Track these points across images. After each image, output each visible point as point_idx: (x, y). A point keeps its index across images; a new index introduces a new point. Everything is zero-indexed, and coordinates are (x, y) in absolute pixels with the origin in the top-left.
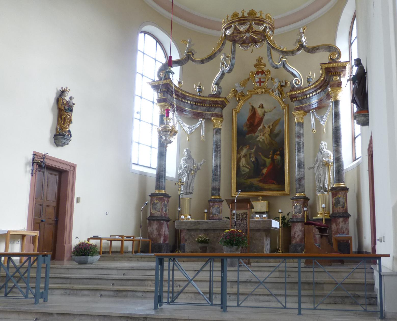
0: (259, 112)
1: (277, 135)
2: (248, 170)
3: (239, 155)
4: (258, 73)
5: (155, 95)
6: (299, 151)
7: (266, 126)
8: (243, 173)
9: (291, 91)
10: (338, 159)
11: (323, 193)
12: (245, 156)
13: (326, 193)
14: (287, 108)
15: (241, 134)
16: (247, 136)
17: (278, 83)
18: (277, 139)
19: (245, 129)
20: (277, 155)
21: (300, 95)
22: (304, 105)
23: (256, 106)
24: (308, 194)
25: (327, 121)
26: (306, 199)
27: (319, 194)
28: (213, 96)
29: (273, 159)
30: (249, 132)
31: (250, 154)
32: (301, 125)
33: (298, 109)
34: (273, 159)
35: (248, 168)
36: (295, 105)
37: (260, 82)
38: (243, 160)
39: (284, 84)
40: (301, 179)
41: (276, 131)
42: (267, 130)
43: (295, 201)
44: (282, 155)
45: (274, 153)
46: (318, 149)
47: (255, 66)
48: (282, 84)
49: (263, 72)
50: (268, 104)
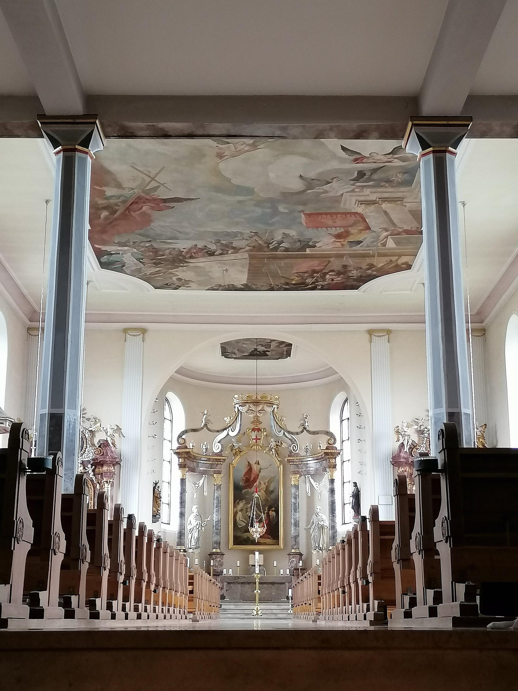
0: (255, 468)
1: (272, 492)
2: (245, 524)
3: (235, 509)
4: (254, 430)
5: (176, 460)
6: (295, 511)
7: (261, 483)
8: (240, 527)
9: (289, 456)
10: (333, 527)
11: (318, 552)
12: (241, 510)
13: (321, 551)
14: (282, 466)
15: (237, 489)
16: (243, 491)
17: (274, 443)
18: (273, 496)
19: (241, 484)
20: (273, 511)
21: (297, 461)
22: (300, 470)
23: (253, 462)
24: (303, 550)
25: (322, 487)
26: (301, 555)
27: (314, 552)
28: (217, 454)
29: (268, 514)
30: (245, 488)
31: (247, 509)
32: (297, 487)
33: (295, 473)
34: (268, 514)
35: (244, 522)
36: (292, 468)
37: (257, 439)
38: (240, 514)
39: (280, 444)
40: (296, 537)
41: (271, 488)
42: (263, 486)
43: (291, 556)
44: (277, 511)
45: (269, 510)
46: (311, 511)
47: (253, 422)
48: (278, 444)
49: (259, 430)
50: (265, 462)
